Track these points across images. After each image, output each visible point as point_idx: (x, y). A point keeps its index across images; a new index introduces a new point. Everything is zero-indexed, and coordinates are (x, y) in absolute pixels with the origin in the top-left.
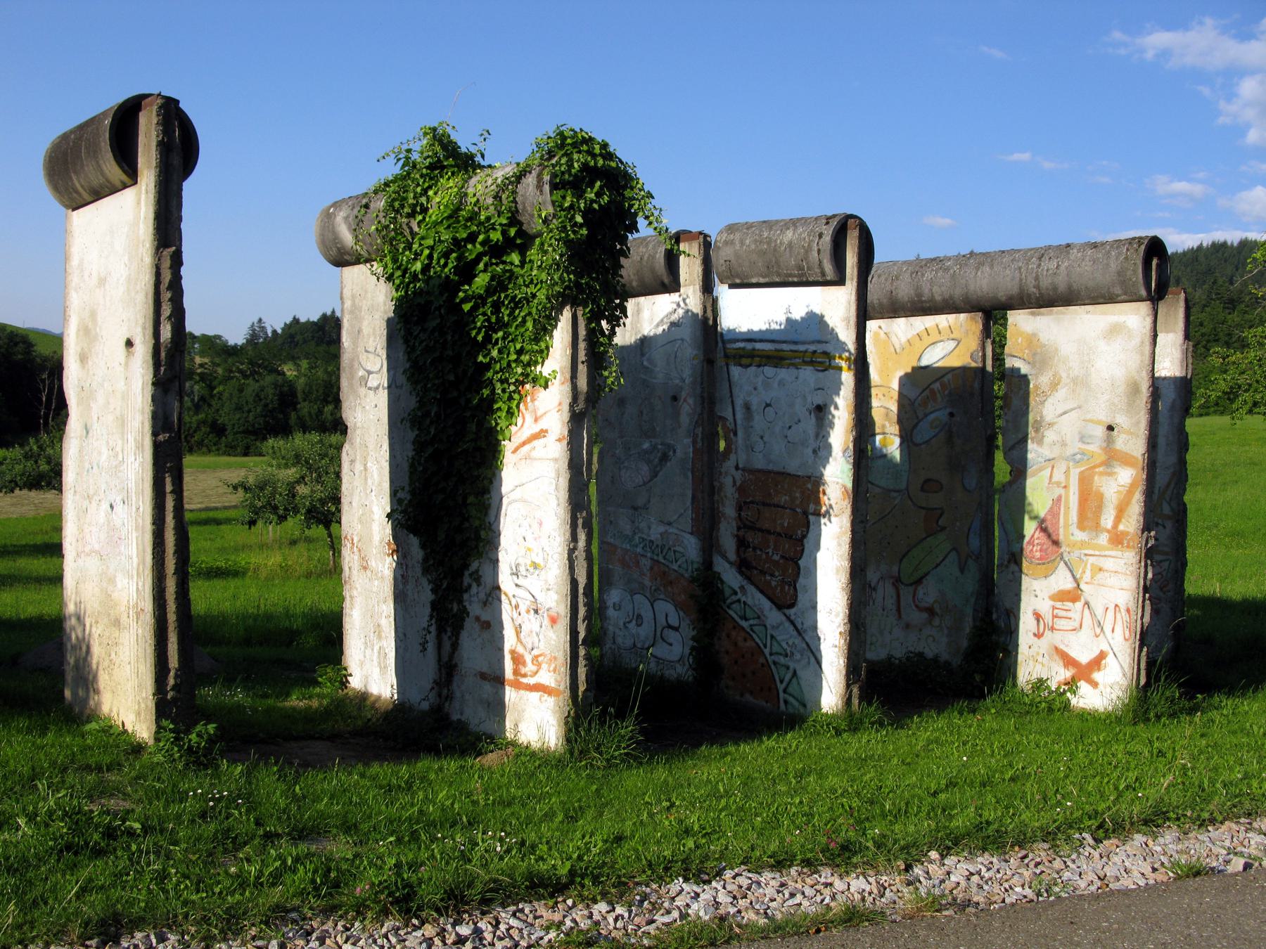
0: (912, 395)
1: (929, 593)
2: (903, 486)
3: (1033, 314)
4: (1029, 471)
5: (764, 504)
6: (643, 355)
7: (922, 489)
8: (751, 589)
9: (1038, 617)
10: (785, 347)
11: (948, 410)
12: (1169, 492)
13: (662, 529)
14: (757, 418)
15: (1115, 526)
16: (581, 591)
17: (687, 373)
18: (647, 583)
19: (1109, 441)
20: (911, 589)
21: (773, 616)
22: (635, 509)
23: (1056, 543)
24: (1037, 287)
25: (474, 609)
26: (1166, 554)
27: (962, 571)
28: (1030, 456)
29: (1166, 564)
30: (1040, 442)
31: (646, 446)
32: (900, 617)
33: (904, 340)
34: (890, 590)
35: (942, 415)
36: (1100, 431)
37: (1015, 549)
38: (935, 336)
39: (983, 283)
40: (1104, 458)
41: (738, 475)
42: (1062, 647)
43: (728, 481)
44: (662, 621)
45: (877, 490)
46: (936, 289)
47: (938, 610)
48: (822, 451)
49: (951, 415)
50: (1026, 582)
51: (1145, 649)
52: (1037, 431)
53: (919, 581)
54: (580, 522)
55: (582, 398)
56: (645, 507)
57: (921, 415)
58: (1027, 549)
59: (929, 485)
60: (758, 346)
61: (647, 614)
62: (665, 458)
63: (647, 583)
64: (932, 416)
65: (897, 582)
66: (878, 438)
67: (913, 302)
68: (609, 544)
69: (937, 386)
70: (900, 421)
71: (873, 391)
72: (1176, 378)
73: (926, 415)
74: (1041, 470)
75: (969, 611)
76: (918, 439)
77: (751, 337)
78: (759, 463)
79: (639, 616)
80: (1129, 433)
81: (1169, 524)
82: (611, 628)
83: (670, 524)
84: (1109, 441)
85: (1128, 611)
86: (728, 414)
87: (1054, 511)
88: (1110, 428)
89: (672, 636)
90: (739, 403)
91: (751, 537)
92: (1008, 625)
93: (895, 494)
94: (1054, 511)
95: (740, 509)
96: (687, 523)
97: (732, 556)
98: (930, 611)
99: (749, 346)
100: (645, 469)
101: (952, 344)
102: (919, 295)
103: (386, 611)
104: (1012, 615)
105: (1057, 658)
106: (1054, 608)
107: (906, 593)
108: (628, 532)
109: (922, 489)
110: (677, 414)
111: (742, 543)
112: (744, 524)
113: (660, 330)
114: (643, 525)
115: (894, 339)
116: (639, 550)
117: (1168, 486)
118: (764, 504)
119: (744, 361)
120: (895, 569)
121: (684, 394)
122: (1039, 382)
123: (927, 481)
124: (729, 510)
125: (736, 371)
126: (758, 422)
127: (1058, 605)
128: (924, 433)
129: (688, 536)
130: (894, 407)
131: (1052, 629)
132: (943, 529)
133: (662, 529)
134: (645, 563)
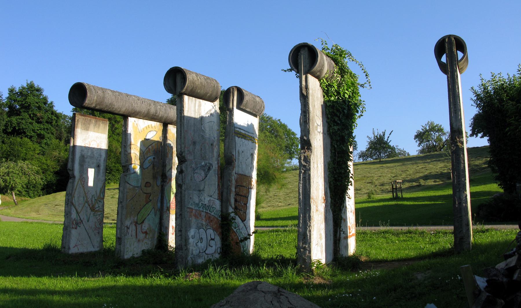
0: (144, 149)
1: (145, 226)
2: (139, 185)
5: (241, 186)
6: (202, 124)
7: (145, 186)
8: (237, 217)
10: (247, 133)
13: (209, 198)
14: (240, 156)
17: (216, 135)
18: (204, 223)
20: (140, 226)
21: (241, 225)
22: (200, 191)
25: (343, 216)
27: (155, 215)
31: (203, 163)
32: (137, 237)
33: (142, 128)
34: (134, 227)
35: (151, 158)
37: (168, 206)
38: (150, 129)
41: (236, 175)
43: (233, 178)
44: (209, 238)
45: (131, 187)
46: (161, 112)
47: (148, 232)
48: (252, 168)
49: (154, 158)
53: (143, 222)
56: (203, 190)
57: (146, 157)
58: (171, 205)
59: (147, 184)
60: (242, 131)
61: (204, 237)
62: (209, 169)
63: (204, 223)
64: (149, 158)
65: (136, 223)
66: (133, 165)
67: (153, 115)
68: (190, 208)
69: (150, 147)
70: (140, 159)
71: (132, 146)
73: (147, 158)
76: (145, 167)
77: (241, 128)
78: (240, 172)
79: (202, 238)
82: (191, 248)
83: (211, 196)
86: (234, 154)
89: (212, 243)
90: (237, 150)
91: (238, 198)
92: (166, 232)
93: (136, 188)
95: (236, 188)
96: (216, 196)
97: (233, 206)
98: (146, 233)
99: (240, 130)
100: (203, 173)
101: (155, 133)
102: (156, 113)
103: (323, 226)
107: (139, 227)
108: (197, 202)
109: (145, 186)
110: (213, 152)
111: (236, 201)
112: (237, 194)
113: (207, 116)
114: (203, 198)
115: (139, 127)
116: (201, 209)
118: (241, 186)
119: (239, 136)
120: (136, 218)
121: (215, 144)
123: (147, 183)
124: (233, 189)
125: (237, 138)
126: (241, 158)
128: (147, 164)
129: (217, 200)
130: (138, 154)
132: (151, 200)
133: (209, 198)
134: (203, 214)
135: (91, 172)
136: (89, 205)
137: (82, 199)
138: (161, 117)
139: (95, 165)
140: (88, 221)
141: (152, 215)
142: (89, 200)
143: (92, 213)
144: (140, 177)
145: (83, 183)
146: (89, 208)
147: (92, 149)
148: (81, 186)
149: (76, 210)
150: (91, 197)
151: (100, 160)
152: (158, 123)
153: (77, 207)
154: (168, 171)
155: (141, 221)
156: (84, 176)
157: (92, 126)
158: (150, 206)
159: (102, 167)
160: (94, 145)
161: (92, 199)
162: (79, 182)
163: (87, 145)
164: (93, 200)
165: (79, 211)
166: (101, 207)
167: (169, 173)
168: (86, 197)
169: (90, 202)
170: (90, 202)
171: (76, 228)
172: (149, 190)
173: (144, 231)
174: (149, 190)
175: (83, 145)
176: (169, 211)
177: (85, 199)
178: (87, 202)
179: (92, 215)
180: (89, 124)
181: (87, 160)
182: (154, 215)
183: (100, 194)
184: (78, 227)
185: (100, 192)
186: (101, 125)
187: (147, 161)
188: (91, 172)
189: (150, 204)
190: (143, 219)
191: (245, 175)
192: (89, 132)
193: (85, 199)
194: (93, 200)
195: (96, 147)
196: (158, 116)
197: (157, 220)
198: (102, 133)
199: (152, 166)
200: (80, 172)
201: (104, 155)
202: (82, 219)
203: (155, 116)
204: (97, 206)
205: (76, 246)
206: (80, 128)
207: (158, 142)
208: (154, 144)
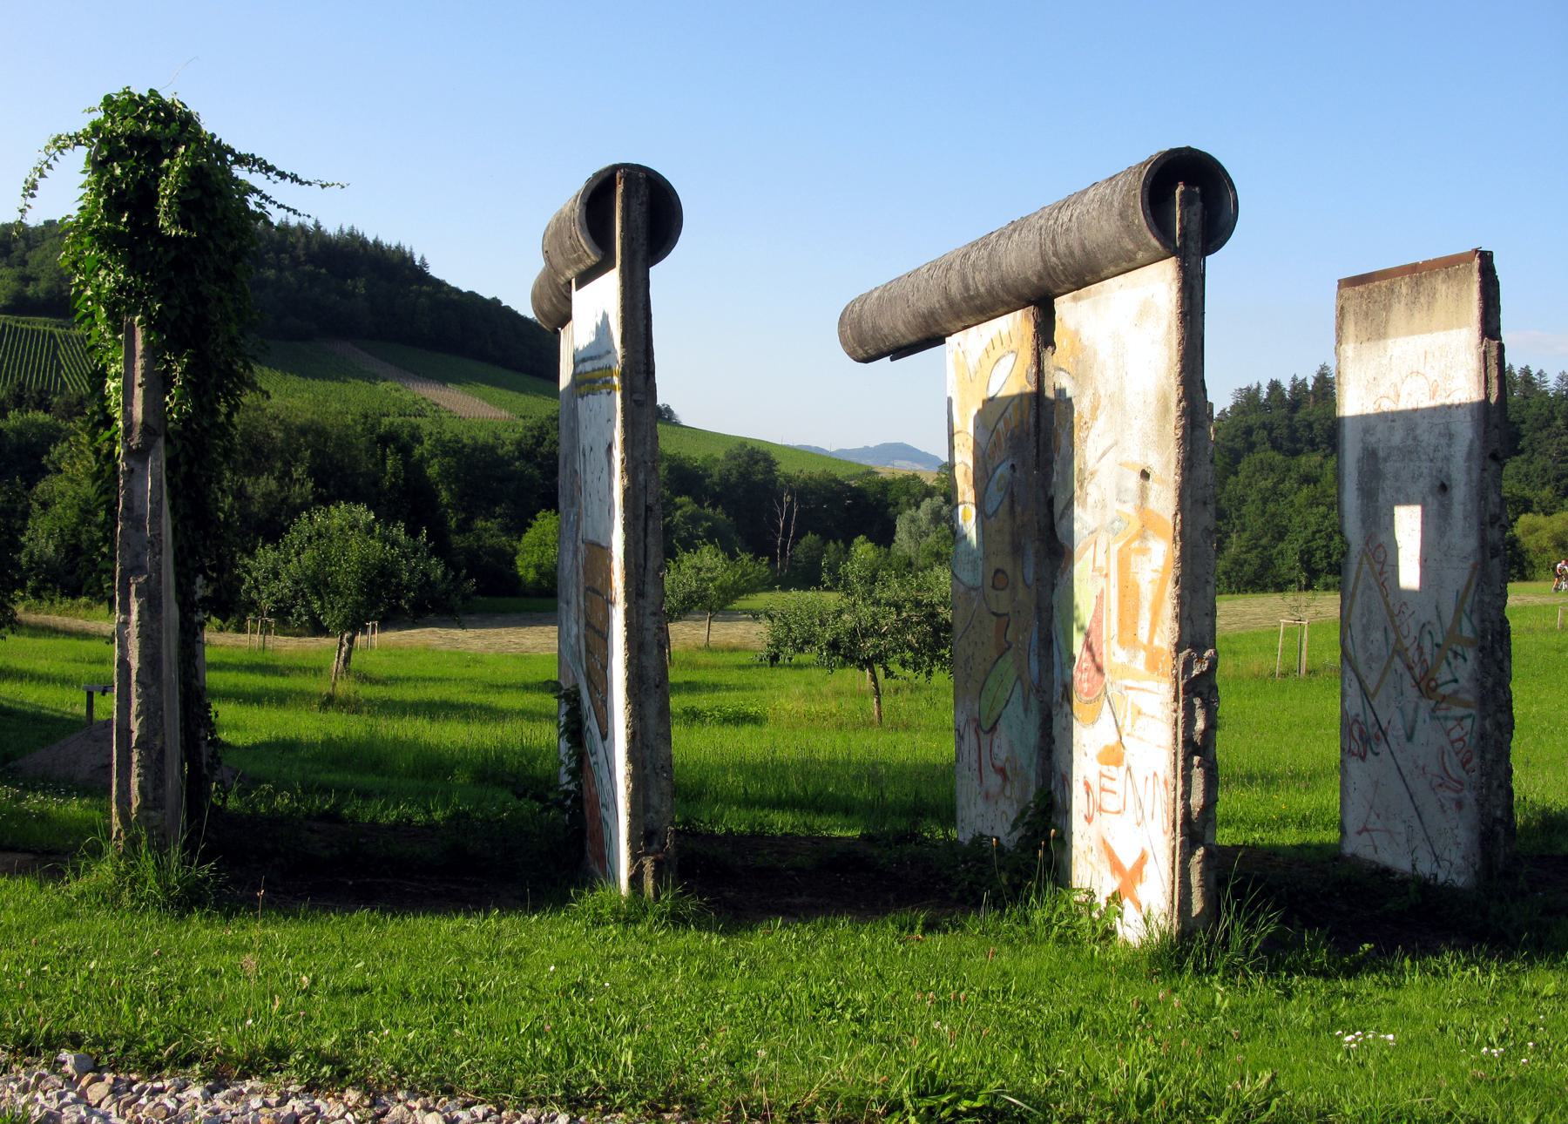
3: (1075, 299)
4: (1076, 550)
7: (994, 587)
9: (1087, 785)
11: (1010, 462)
12: (1469, 600)
15: (1151, 641)
16: (134, 677)
19: (1143, 495)
20: (988, 737)
23: (1099, 669)
24: (1056, 254)
26: (1467, 705)
27: (1026, 710)
28: (1077, 527)
29: (1468, 722)
30: (1084, 505)
36: (1134, 480)
39: (1020, 260)
40: (1136, 526)
42: (1109, 840)
50: (1078, 729)
51: (1200, 852)
52: (1081, 486)
53: (993, 728)
54: (133, 588)
55: (137, 430)
64: (999, 471)
72: (1472, 404)
73: (994, 470)
74: (1086, 548)
75: (1033, 775)
76: (989, 509)
80: (1163, 482)
81: (1471, 654)
84: (1143, 495)
85: (1166, 783)
87: (1097, 618)
88: (1145, 475)
93: (973, 594)
94: (1097, 618)
101: (1011, 358)
104: (1066, 781)
105: (1105, 857)
106: (1102, 775)
117: (1467, 588)
122: (1082, 407)
127: (1104, 769)
131: (1100, 809)
135: (1408, 524)
136: (1410, 668)
137: (1377, 635)
138: (990, 291)
139: (1424, 484)
140: (1409, 738)
141: (1014, 711)
142: (1407, 643)
143: (1426, 705)
144: (980, 554)
145: (1377, 567)
146: (1408, 681)
147: (1409, 419)
148: (1372, 581)
149: (1361, 682)
150: (1414, 632)
151: (1447, 459)
152: (1019, 312)
153: (1362, 669)
154: (1061, 518)
155: (991, 722)
156: (1382, 538)
157: (1399, 310)
158: (1007, 666)
159: (1460, 492)
160: (1415, 397)
161: (1419, 640)
162: (1366, 567)
163: (1388, 406)
164: (1427, 644)
165: (1371, 689)
166: (1462, 682)
167: (1064, 522)
168: (1396, 629)
169: (1412, 654)
170: (1412, 654)
171: (1363, 758)
172: (1002, 602)
173: (999, 763)
174: (1002, 602)
175: (1370, 409)
176: (1070, 701)
177: (1392, 636)
178: (1400, 652)
179: (1423, 714)
180: (1387, 308)
181: (1389, 468)
182: (1020, 709)
183: (1457, 620)
184: (1370, 755)
185: (1458, 610)
186: (1442, 288)
187: (993, 487)
188: (1408, 524)
189: (1009, 657)
190: (995, 714)
191: (599, 545)
192: (1389, 342)
193: (1392, 636)
194: (1427, 644)
195: (1426, 403)
196: (978, 295)
197: (1033, 737)
198: (1448, 327)
199: (1006, 502)
200: (1363, 522)
201: (1465, 433)
202: (1384, 725)
203: (972, 298)
204: (1444, 674)
205: (1365, 829)
206: (1352, 338)
207: (1021, 396)
208: (1010, 410)
